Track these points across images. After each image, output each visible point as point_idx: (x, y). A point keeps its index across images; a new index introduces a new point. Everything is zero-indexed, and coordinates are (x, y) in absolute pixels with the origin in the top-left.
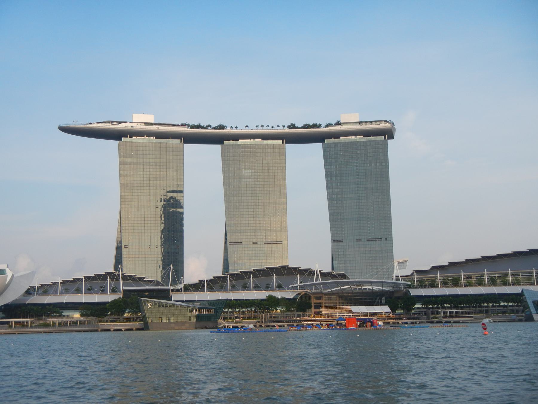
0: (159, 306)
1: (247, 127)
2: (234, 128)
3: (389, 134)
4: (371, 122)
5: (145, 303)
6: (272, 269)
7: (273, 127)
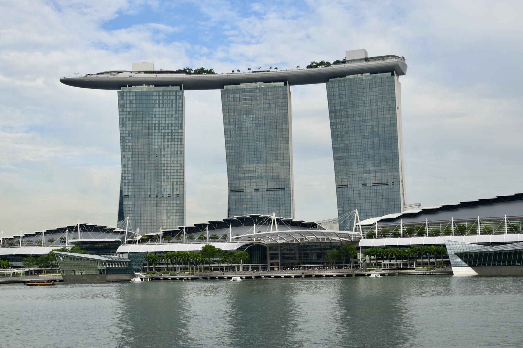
0: (71, 259)
1: (249, 69)
2: (236, 72)
3: (395, 69)
4: (377, 58)
5: (57, 257)
6: (241, 219)
7: (276, 68)
